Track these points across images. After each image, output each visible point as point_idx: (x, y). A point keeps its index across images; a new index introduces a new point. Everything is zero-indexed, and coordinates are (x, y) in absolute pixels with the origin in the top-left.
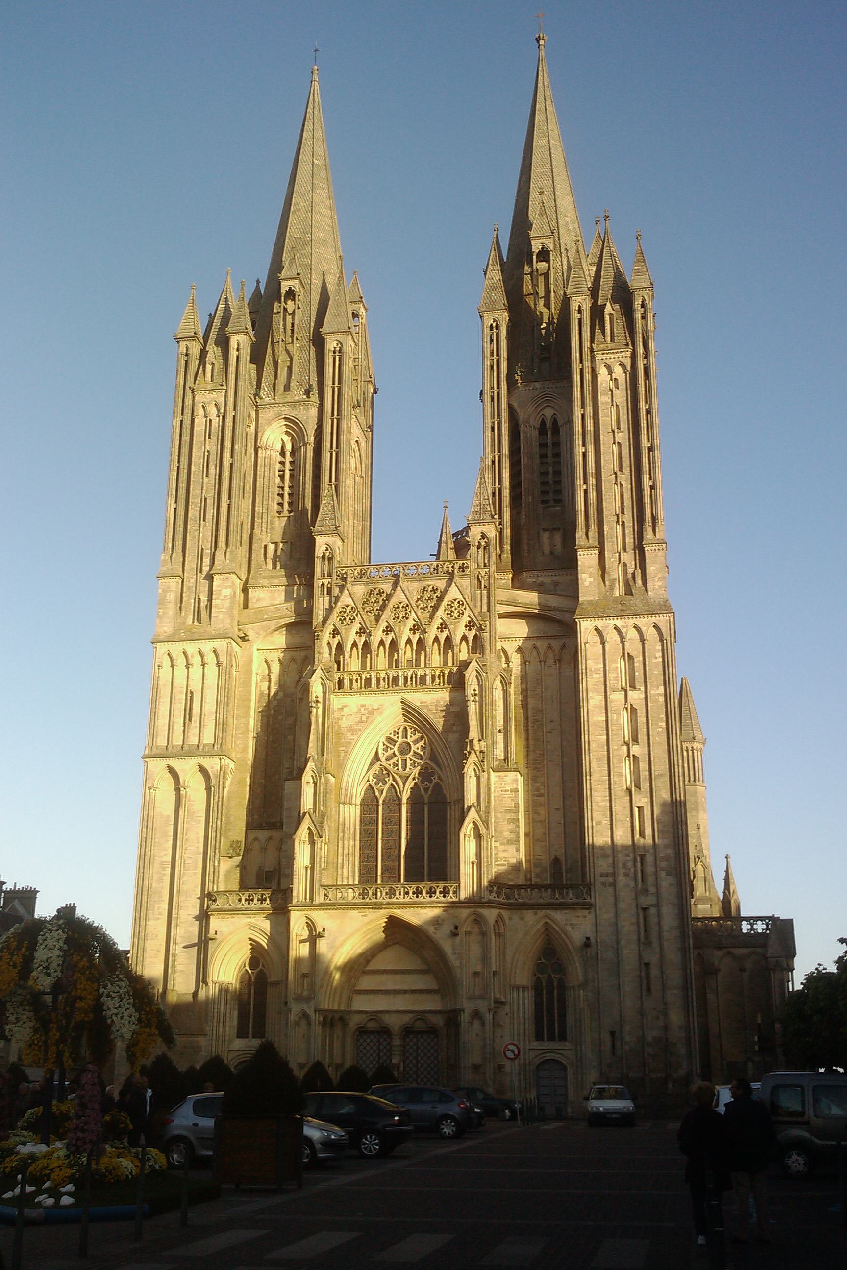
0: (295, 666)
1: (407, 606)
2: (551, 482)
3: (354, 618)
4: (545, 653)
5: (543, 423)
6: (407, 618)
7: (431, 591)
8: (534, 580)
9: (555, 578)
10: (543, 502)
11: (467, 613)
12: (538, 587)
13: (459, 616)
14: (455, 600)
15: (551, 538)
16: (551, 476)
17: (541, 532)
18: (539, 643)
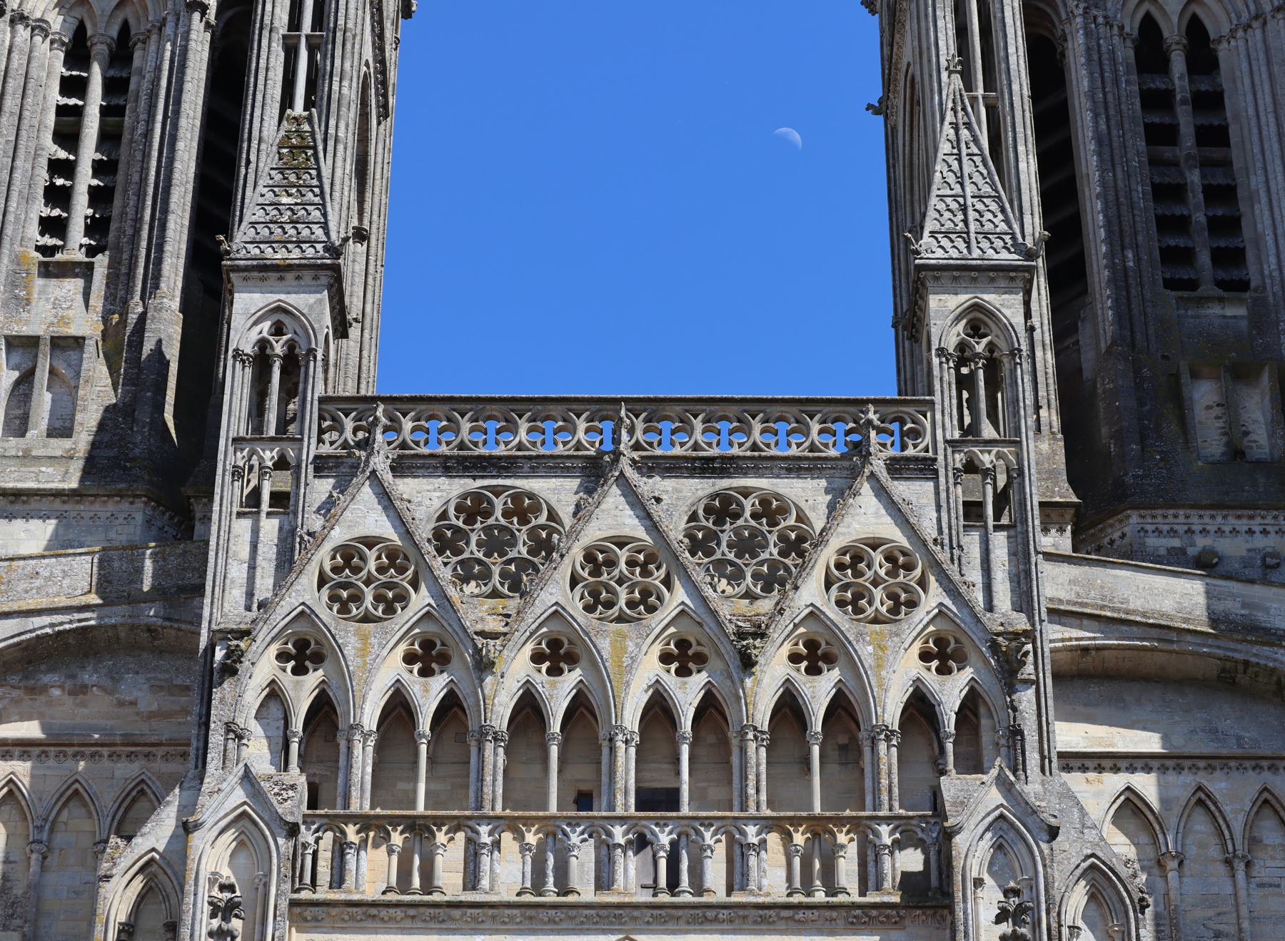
0: (86, 825)
1: (651, 558)
2: (1199, 217)
3: (403, 598)
4: (1249, 825)
5: (1149, 25)
6: (651, 609)
7: (755, 516)
8: (1176, 543)
9: (1260, 542)
10: (1170, 284)
11: (934, 597)
12: (1206, 565)
13: (894, 611)
14: (875, 544)
15: (1229, 406)
16: (1196, 197)
17: (1185, 378)
18: (1218, 785)
